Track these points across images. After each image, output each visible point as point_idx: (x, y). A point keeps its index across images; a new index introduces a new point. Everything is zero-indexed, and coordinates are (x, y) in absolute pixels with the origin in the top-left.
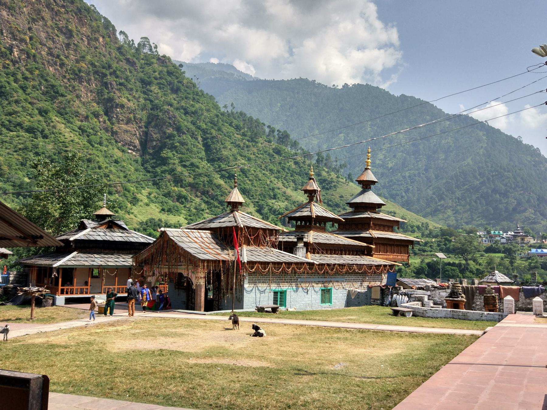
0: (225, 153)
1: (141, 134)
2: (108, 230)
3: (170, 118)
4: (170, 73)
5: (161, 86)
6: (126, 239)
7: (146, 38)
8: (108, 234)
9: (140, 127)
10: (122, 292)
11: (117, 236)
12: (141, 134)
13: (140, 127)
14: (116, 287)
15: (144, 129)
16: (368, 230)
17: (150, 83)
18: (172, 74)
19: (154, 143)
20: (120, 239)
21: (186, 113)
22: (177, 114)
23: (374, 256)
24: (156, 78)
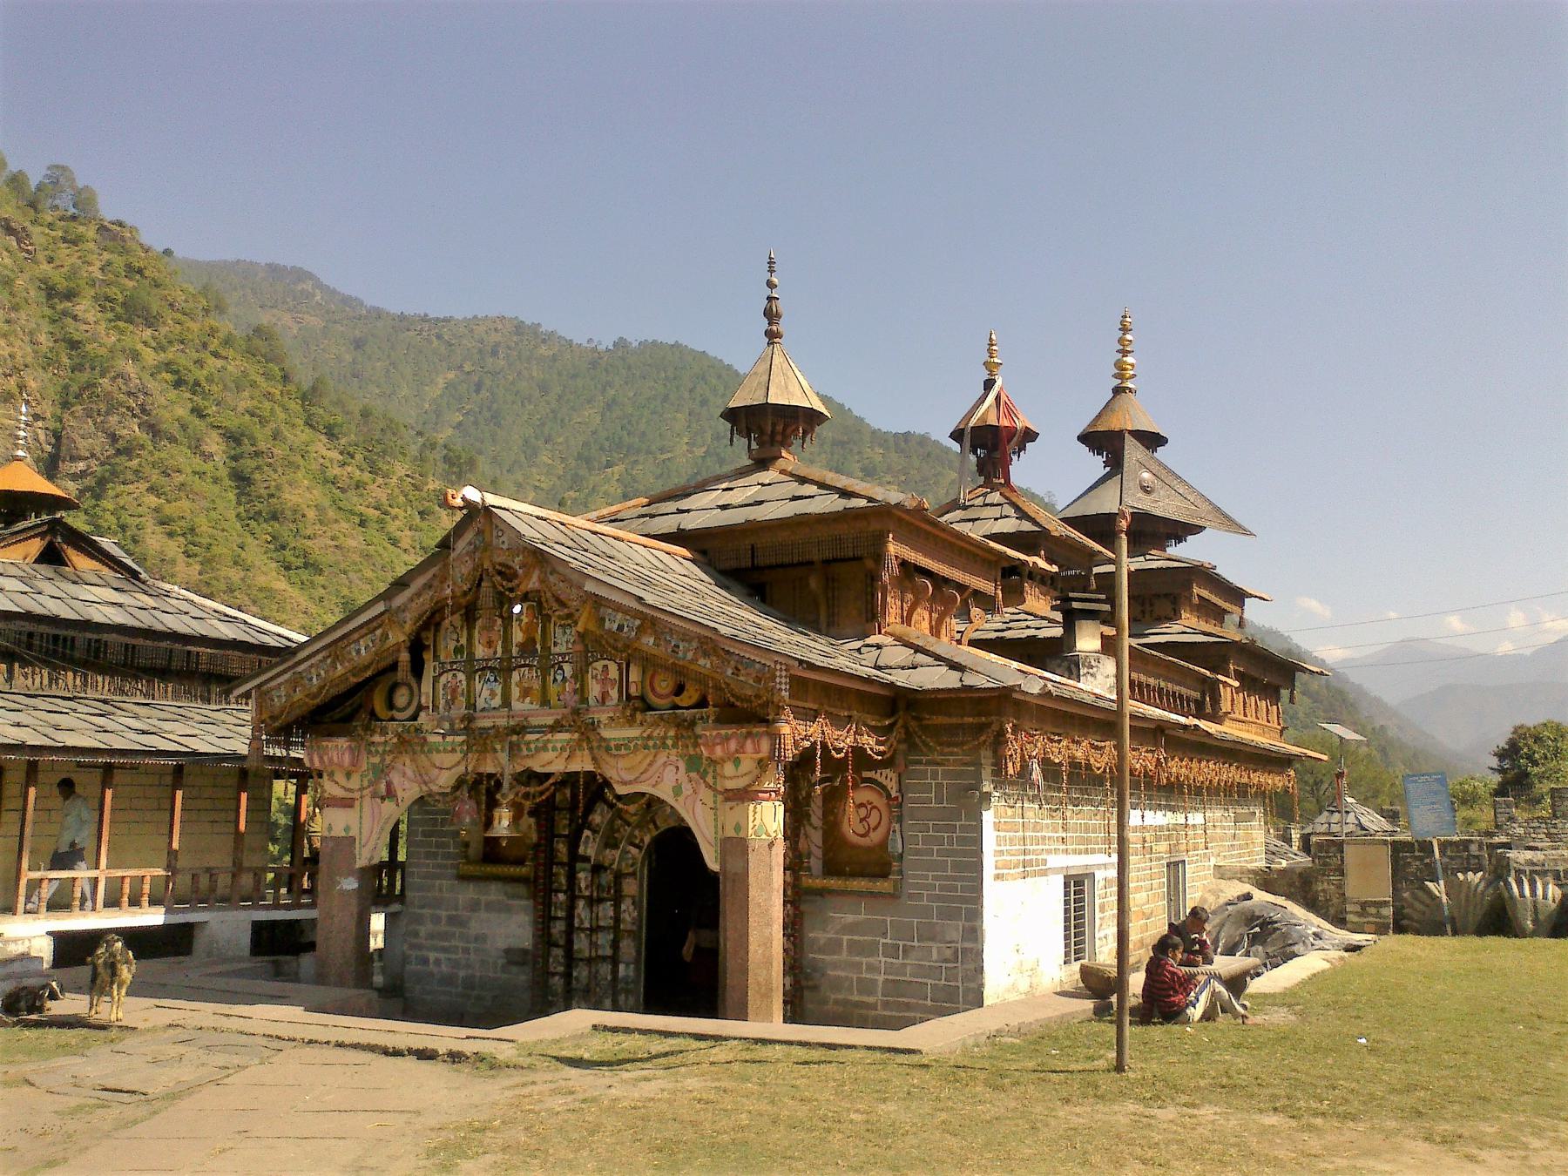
0: (291, 497)
1: (42, 437)
2: (45, 570)
3: (129, 394)
4: (133, 271)
5: (104, 302)
6: (146, 620)
7: (64, 168)
8: (48, 588)
9: (37, 417)
10: (135, 902)
11: (93, 598)
12: (42, 437)
13: (37, 417)
14: (102, 874)
15: (52, 425)
16: (1174, 616)
17: (70, 295)
18: (140, 271)
19: (81, 466)
20: (117, 617)
21: (178, 384)
22: (152, 385)
23: (1227, 722)
24: (92, 283)
